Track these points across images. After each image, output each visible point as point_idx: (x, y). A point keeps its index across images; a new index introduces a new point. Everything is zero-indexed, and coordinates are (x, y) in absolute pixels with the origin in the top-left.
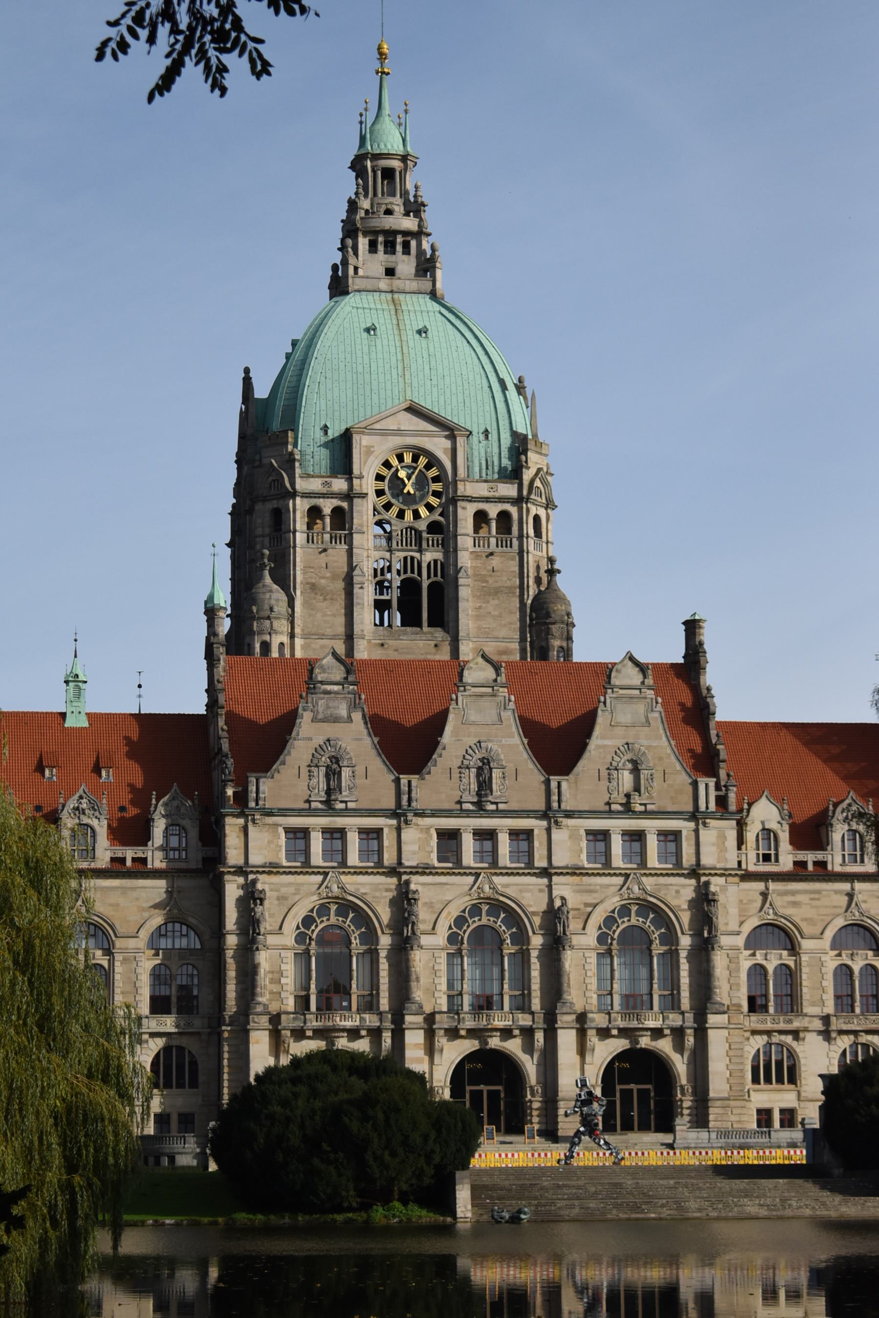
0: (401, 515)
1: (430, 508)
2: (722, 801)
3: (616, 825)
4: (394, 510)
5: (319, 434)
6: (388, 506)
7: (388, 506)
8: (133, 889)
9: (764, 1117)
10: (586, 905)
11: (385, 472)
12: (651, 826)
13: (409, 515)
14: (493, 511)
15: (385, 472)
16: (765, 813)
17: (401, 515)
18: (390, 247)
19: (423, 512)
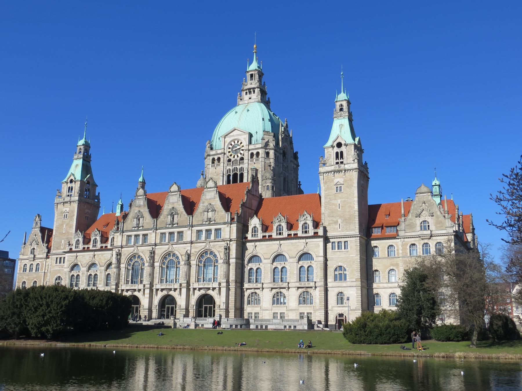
0: (234, 157)
1: (241, 154)
2: (232, 219)
3: (204, 228)
4: (233, 156)
5: (218, 139)
6: (231, 155)
7: (231, 155)
8: (102, 254)
9: (275, 315)
10: (195, 252)
11: (230, 146)
12: (213, 227)
13: (236, 156)
14: (255, 152)
15: (230, 146)
16: (255, 222)
17: (234, 157)
18: (250, 93)
19: (239, 155)
